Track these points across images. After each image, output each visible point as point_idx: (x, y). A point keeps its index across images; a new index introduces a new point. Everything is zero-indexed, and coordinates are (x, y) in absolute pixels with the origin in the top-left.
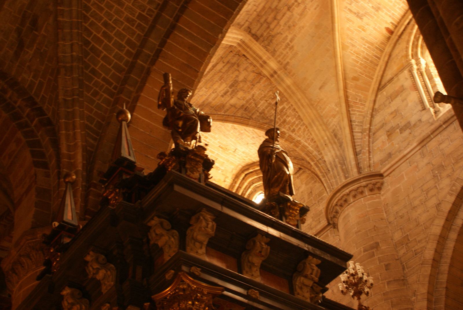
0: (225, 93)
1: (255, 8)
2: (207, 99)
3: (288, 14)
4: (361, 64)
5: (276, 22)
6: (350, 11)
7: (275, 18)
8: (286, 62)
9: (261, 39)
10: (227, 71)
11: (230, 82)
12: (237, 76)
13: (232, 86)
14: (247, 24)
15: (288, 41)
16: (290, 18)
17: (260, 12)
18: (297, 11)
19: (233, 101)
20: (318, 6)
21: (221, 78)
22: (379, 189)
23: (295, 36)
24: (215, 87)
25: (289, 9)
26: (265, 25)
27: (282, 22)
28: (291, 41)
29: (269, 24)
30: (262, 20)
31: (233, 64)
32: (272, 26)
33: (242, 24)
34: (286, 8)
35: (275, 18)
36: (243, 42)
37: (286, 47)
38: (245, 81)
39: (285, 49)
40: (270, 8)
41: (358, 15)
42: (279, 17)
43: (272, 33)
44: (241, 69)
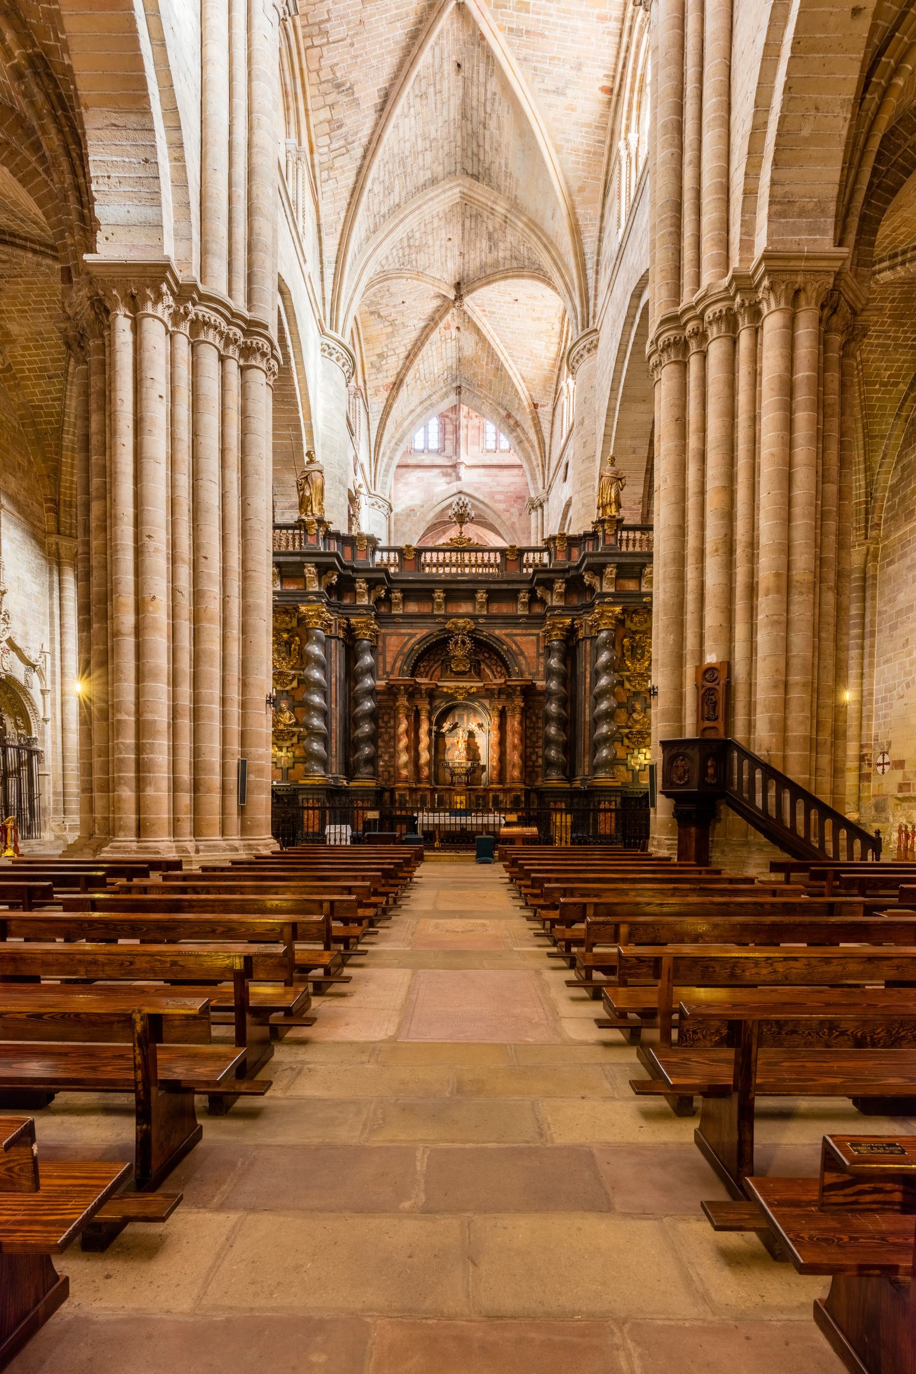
0: (490, 249)
1: (453, 144)
2: (481, 260)
3: (487, 133)
4: (583, 164)
5: (481, 149)
6: (547, 91)
7: (479, 146)
8: (513, 197)
9: (481, 177)
10: (476, 225)
11: (485, 236)
12: (487, 228)
13: (490, 239)
14: (459, 166)
15: (504, 168)
16: (491, 138)
17: (462, 144)
18: (492, 124)
19: (501, 254)
20: (508, 106)
21: (476, 234)
22: (596, 347)
23: (506, 158)
24: (478, 245)
25: (485, 128)
26: (475, 159)
27: (487, 148)
28: (506, 167)
29: (477, 155)
30: (470, 153)
31: (476, 216)
32: (482, 157)
33: (453, 169)
34: (481, 126)
35: (479, 146)
36: (463, 193)
37: (506, 176)
38: (495, 230)
39: (506, 180)
40: (468, 134)
41: (558, 92)
42: (481, 143)
43: (487, 166)
44: (485, 219)
